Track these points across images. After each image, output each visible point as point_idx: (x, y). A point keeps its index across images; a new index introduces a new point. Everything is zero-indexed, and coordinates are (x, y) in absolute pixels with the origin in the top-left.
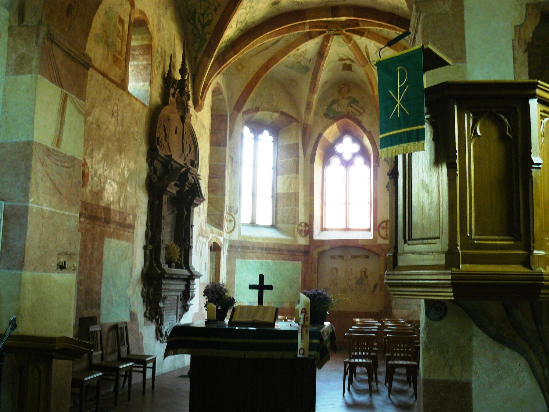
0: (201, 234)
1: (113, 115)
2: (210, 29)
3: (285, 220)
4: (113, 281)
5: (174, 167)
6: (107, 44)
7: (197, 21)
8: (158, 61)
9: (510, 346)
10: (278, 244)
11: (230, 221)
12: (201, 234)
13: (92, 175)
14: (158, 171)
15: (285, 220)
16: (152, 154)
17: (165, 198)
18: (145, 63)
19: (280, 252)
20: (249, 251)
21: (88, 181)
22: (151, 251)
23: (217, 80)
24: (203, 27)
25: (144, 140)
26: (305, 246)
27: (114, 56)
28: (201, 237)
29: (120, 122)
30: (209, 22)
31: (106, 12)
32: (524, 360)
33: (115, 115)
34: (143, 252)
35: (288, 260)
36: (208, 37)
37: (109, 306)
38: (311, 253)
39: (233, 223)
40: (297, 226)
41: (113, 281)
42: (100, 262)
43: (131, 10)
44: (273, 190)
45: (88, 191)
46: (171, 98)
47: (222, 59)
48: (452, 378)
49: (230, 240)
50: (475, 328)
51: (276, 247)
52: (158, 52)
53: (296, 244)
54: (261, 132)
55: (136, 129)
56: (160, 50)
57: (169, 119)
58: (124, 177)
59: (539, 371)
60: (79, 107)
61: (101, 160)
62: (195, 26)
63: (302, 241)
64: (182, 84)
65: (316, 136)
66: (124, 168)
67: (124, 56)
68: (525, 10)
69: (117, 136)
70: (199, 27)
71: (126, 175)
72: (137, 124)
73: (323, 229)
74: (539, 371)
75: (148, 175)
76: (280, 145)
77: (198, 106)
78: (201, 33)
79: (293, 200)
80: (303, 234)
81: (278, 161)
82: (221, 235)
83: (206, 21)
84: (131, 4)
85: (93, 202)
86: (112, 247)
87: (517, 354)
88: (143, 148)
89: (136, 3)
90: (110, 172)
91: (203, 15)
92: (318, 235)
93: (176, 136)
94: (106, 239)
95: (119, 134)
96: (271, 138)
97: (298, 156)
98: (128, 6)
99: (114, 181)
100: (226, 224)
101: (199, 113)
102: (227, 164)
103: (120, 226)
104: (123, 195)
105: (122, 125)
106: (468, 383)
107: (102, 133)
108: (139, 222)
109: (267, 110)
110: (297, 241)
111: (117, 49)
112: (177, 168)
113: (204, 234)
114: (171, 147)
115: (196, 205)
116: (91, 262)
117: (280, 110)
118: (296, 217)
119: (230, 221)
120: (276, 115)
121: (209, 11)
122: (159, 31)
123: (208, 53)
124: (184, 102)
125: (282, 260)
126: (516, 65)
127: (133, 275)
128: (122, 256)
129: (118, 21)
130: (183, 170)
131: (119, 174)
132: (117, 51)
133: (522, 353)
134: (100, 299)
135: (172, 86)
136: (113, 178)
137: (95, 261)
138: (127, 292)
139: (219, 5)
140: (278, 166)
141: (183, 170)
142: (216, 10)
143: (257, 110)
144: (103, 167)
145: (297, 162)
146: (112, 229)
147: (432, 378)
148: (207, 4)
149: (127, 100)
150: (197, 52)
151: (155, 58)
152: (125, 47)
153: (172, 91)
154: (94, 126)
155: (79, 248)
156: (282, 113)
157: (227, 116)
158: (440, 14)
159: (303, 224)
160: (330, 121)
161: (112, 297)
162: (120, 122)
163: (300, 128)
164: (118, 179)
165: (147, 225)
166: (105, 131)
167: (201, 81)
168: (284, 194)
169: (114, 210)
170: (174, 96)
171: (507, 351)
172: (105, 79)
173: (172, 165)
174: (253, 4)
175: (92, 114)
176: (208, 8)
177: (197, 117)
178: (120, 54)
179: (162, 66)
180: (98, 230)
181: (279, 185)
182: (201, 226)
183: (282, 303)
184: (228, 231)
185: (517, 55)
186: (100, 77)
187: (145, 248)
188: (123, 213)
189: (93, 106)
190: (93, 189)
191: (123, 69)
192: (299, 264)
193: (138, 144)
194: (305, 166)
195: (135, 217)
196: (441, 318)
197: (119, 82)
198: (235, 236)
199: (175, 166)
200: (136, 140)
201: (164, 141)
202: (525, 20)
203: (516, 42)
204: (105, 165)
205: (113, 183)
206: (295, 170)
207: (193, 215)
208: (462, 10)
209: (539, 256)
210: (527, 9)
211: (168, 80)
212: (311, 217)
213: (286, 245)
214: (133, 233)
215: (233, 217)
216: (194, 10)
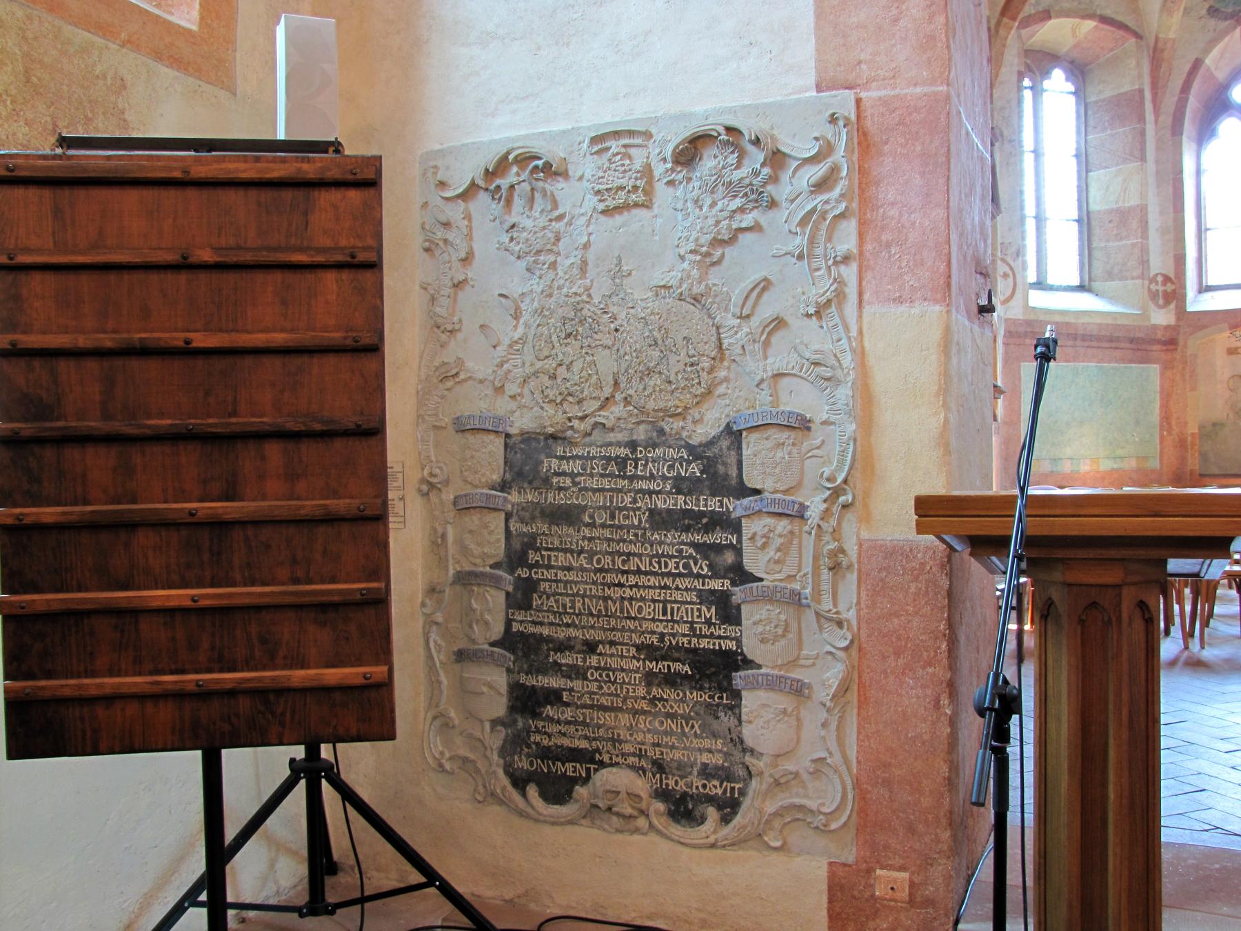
3: (1116, 271)
10: (1108, 325)
15: (1116, 271)
19: (1113, 345)
26: (1167, 327)
35: (1131, 361)
38: (1181, 342)
39: (1011, 279)
40: (1147, 282)
44: (1080, 208)
49: (1006, 320)
51: (1103, 333)
53: (1147, 324)
54: (1046, 74)
63: (1162, 317)
65: (1187, 67)
73: (1203, 289)
76: (1092, 98)
79: (1134, 224)
80: (1161, 302)
81: (1090, 137)
92: (1198, 303)
96: (1071, 87)
97: (1142, 119)
109: (1067, 14)
110: (1149, 319)
117: (1099, 12)
118: (1144, 263)
120: (1090, 24)
125: (1116, 362)
140: (1090, 150)
143: (1046, 15)
145: (1143, 133)
156: (1104, 20)
159: (1160, 279)
160: (1223, 25)
163: (1145, 53)
168: (1110, 212)
181: (1094, 193)
183: (1145, 458)
192: (1156, 368)
194: (1159, 141)
206: (1137, 153)
212: (1180, 260)
213: (1124, 326)
215: (1011, 268)
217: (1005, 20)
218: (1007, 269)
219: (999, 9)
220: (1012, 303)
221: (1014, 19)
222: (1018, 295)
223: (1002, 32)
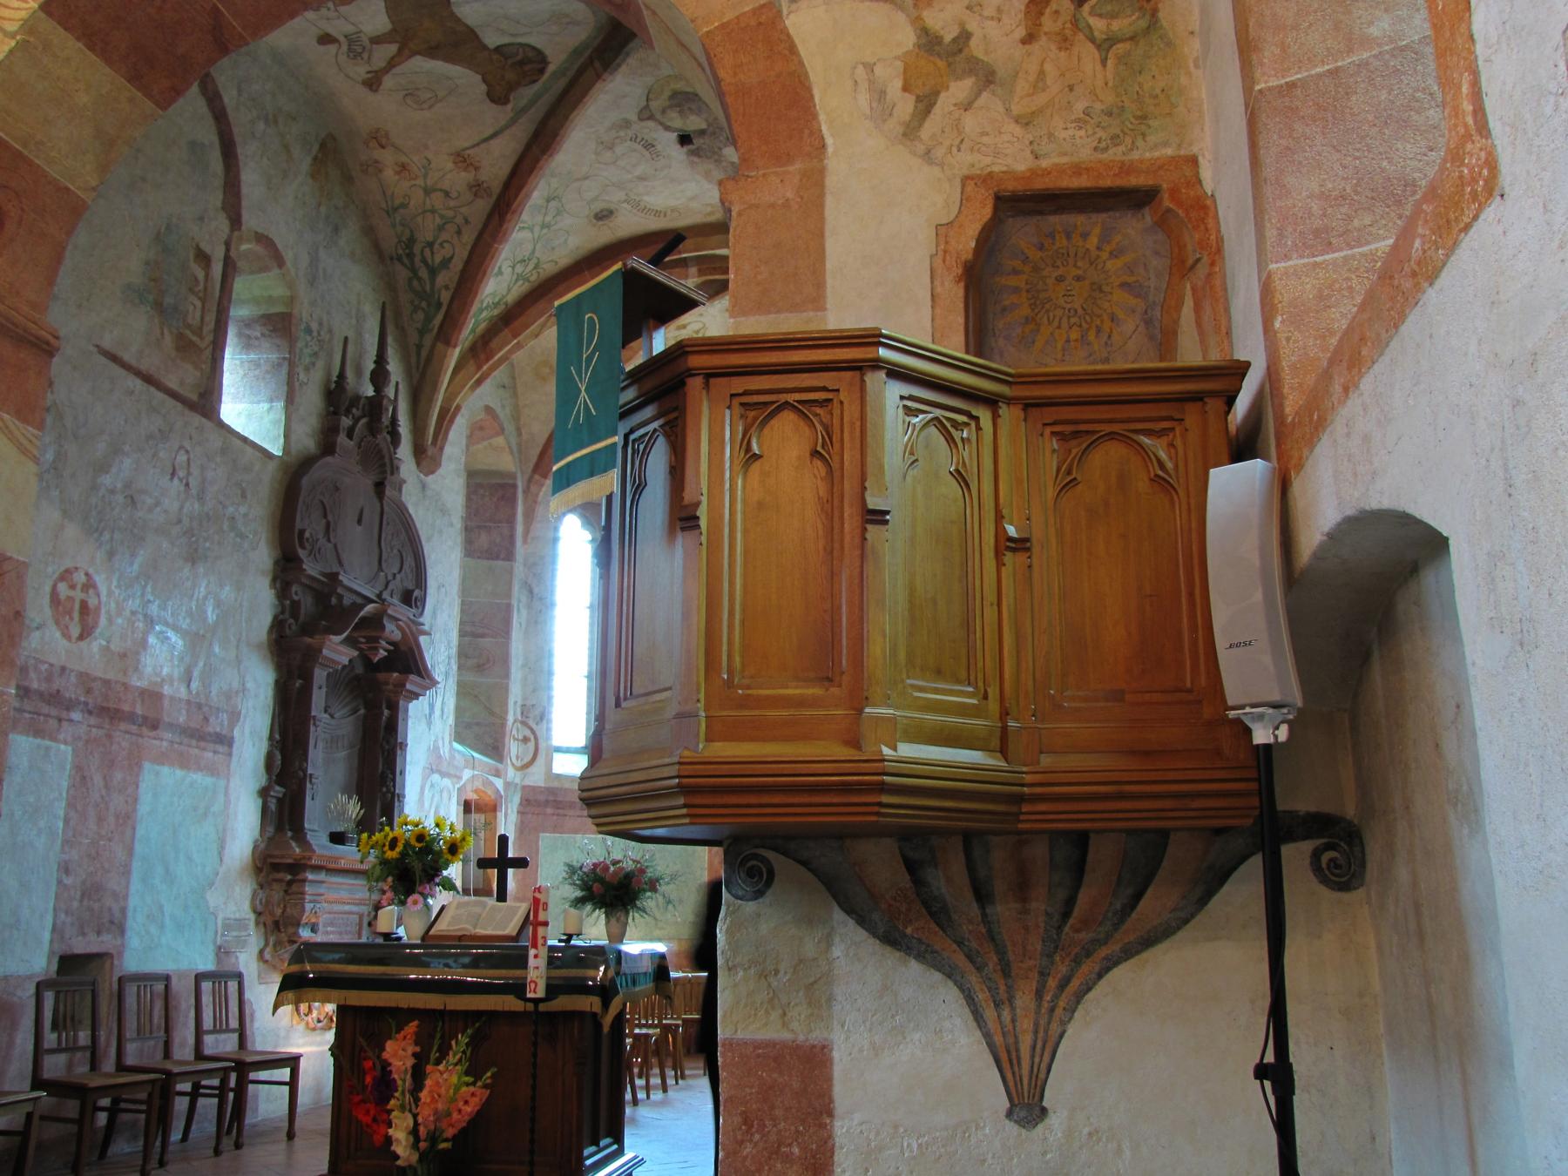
0: (436, 767)
1: (173, 474)
2: (447, 278)
4: (167, 871)
5: (347, 601)
6: (159, 307)
7: (417, 259)
8: (307, 351)
9: (920, 957)
11: (525, 740)
12: (436, 767)
13: (108, 612)
14: (303, 611)
16: (286, 568)
17: (320, 675)
18: (274, 356)
20: (571, 812)
21: (96, 624)
22: (279, 800)
23: (477, 400)
24: (433, 272)
25: (264, 536)
27: (180, 337)
28: (436, 777)
29: (194, 492)
30: (446, 263)
31: (159, 233)
32: (955, 991)
33: (181, 474)
34: (260, 801)
36: (445, 297)
37: (153, 930)
39: (531, 745)
41: (167, 871)
42: (127, 819)
43: (232, 230)
45: (95, 650)
46: (342, 439)
47: (481, 349)
48: (786, 1036)
49: (524, 788)
50: (838, 915)
52: (309, 331)
55: (243, 510)
56: (314, 326)
57: (337, 489)
58: (205, 619)
59: (989, 1013)
60: (25, 442)
61: (137, 578)
62: (414, 270)
64: (374, 407)
66: (205, 598)
67: (210, 338)
68: (959, 190)
69: (186, 521)
70: (423, 273)
71: (211, 615)
72: (244, 496)
74: (989, 1013)
75: (275, 617)
77: (426, 456)
78: (428, 288)
82: (497, 774)
83: (438, 259)
84: (230, 219)
85: (110, 676)
86: (163, 789)
87: (938, 976)
88: (263, 556)
89: (245, 216)
90: (163, 607)
91: (431, 245)
93: (359, 529)
94: (147, 765)
95: (191, 519)
98: (222, 224)
99: (176, 628)
100: (513, 749)
101: (430, 478)
102: (514, 603)
103: (192, 736)
104: (201, 664)
105: (200, 498)
106: (824, 1047)
107: (140, 514)
108: (247, 731)
111: (190, 321)
112: (354, 604)
113: (444, 768)
114: (344, 556)
115: (416, 696)
116: (101, 820)
119: (525, 740)
121: (444, 236)
122: (312, 282)
123: (446, 334)
124: (380, 451)
126: (938, 311)
127: (225, 859)
128: (195, 810)
129: (192, 257)
130: (370, 608)
131: (190, 613)
132: (189, 326)
133: (950, 973)
134: (124, 911)
135: (348, 412)
136: (170, 620)
137: (112, 820)
138: (208, 895)
139: (467, 221)
141: (370, 608)
142: (459, 232)
144: (143, 595)
146: (165, 744)
147: (740, 1035)
148: (438, 220)
149: (215, 441)
150: (422, 333)
151: (300, 344)
152: (211, 318)
153: (346, 422)
154: (120, 498)
155: (65, 784)
157: (514, 486)
158: (772, 206)
161: (161, 907)
162: (194, 492)
164: (184, 624)
165: (271, 738)
166: (150, 510)
167: (431, 400)
169: (172, 698)
170: (350, 436)
171: (914, 966)
172: (152, 389)
173: (340, 597)
174: (548, 219)
175: (114, 470)
176: (441, 228)
177: (424, 486)
178: (199, 332)
179: (320, 364)
180: (124, 744)
182: (436, 748)
184: (519, 764)
185: (939, 290)
186: (138, 384)
187: (264, 793)
188: (199, 706)
189: (116, 450)
190: (112, 647)
191: (206, 367)
193: (246, 545)
195: (235, 716)
196: (758, 894)
197: (194, 397)
198: (536, 778)
199: (348, 600)
200: (242, 536)
201: (322, 541)
202: (960, 212)
203: (939, 260)
204: (149, 589)
205: (171, 634)
207: (406, 720)
208: (821, 196)
209: (879, 720)
210: (963, 186)
211: (336, 396)
214: (230, 755)
216: (407, 232)
217: (537, 477)
218: (528, 733)
219: (531, 465)
220: (533, 769)
221: (545, 476)
222: (541, 761)
223: (533, 488)
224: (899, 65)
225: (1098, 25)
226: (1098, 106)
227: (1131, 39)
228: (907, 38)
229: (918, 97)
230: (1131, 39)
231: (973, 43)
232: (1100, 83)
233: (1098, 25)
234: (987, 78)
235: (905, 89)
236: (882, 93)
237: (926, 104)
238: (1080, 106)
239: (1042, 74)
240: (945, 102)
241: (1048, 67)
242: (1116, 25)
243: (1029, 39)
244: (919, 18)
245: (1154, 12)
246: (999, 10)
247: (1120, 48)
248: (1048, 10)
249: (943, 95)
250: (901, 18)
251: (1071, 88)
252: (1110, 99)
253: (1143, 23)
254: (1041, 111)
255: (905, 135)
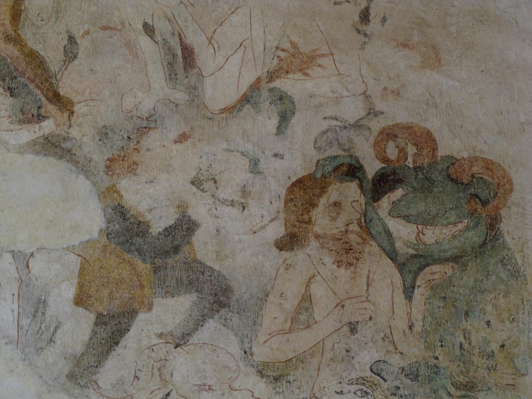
224: (74, 261)
225: (403, 232)
226: (396, 361)
227: (455, 259)
228: (90, 220)
229: (99, 316)
230: (455, 259)
231: (199, 238)
232: (401, 324)
233: (403, 232)
234: (217, 297)
235: (80, 300)
236: (40, 306)
237: (112, 329)
238: (366, 357)
239: (306, 301)
240: (145, 329)
241: (318, 290)
242: (431, 235)
243: (289, 242)
244: (112, 189)
245: (494, 223)
246: (244, 191)
247: (437, 272)
248: (323, 201)
249: (141, 316)
250: (82, 185)
251: (353, 328)
252: (415, 351)
253: (475, 237)
254: (301, 360)
255: (71, 376)
